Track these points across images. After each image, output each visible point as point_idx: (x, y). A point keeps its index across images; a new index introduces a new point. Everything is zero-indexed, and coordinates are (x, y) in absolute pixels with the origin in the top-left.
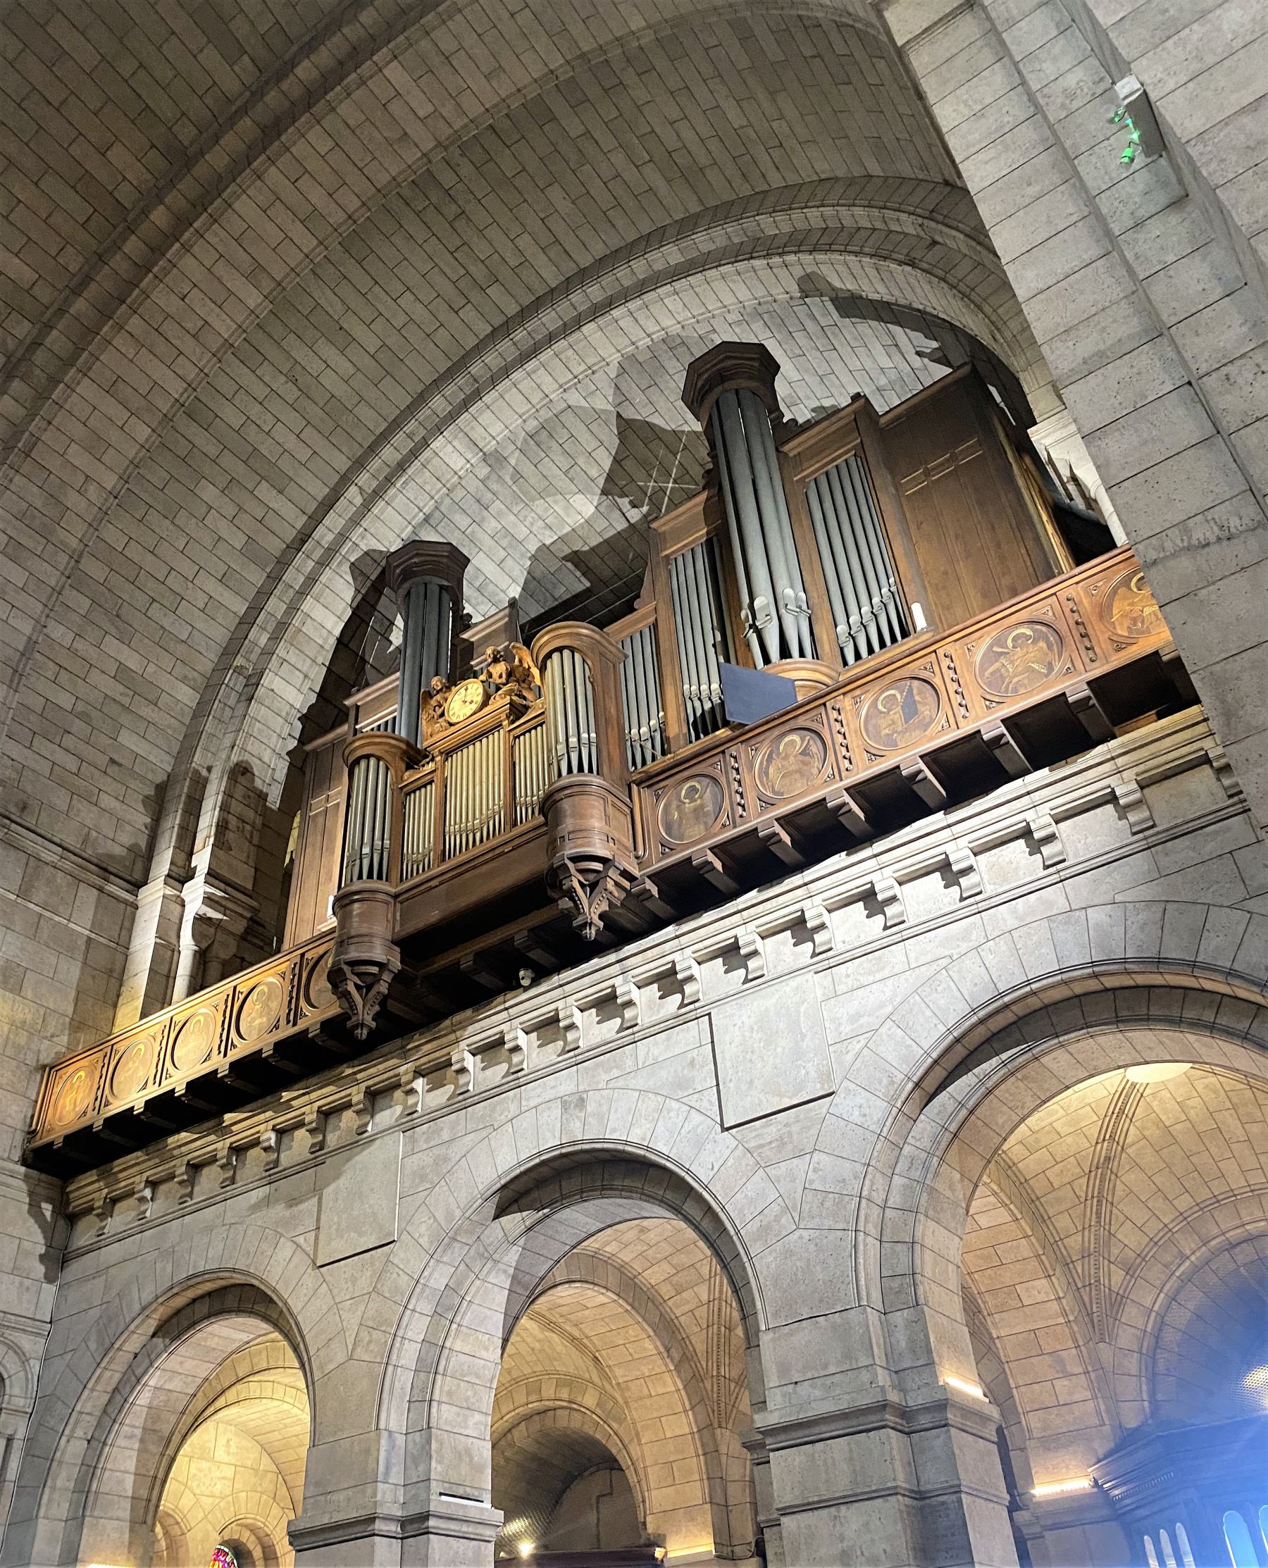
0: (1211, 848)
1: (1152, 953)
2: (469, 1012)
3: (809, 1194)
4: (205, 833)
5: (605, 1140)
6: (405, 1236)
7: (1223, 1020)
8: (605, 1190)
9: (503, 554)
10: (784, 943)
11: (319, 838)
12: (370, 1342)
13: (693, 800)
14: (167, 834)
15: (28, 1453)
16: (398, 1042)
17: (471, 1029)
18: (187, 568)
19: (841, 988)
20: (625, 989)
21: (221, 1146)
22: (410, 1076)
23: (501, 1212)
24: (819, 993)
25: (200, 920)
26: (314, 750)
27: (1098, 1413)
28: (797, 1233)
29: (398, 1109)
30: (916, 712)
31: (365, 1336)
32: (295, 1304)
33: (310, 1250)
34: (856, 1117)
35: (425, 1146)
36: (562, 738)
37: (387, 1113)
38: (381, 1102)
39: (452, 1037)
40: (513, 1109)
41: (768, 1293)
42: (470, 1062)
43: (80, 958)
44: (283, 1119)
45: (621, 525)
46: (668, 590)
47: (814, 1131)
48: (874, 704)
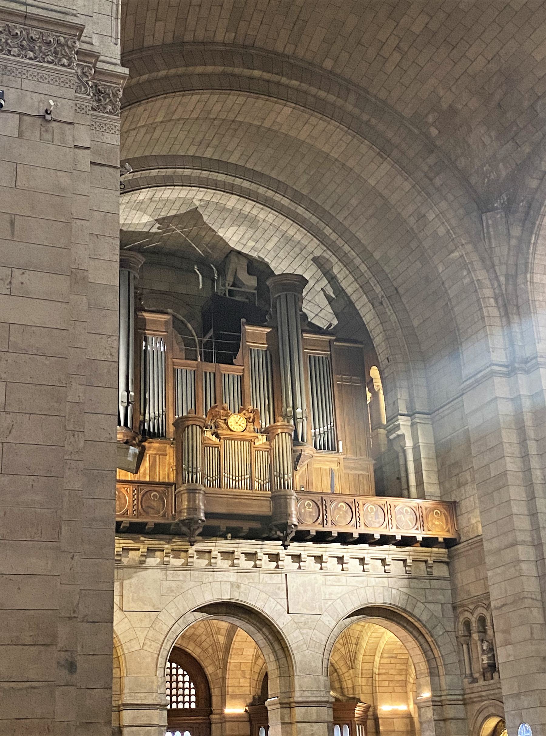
0: (421, 586)
1: (404, 607)
3: (312, 642)
5: (247, 603)
6: (164, 610)
7: (408, 627)
8: (234, 615)
10: (311, 560)
12: (150, 645)
13: (309, 508)
16: (168, 537)
19: (327, 583)
20: (260, 555)
23: (193, 611)
24: (321, 582)
27: (250, 691)
28: (307, 651)
29: (158, 560)
30: (378, 518)
31: (148, 642)
34: (327, 623)
35: (172, 579)
40: (211, 580)
41: (298, 665)
47: (315, 623)
48: (368, 507)
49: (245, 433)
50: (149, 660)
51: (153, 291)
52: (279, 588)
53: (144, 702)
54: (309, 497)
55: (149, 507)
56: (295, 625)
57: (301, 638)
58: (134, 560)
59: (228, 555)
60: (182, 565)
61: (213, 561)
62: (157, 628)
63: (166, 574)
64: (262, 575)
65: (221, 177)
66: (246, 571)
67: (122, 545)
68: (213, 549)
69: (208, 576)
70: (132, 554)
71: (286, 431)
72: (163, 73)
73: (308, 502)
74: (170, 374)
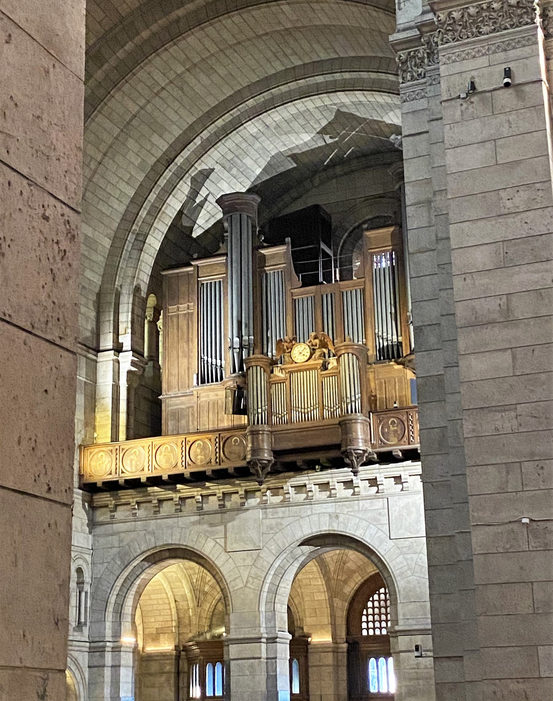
2: (291, 474)
3: (417, 567)
4: (125, 325)
6: (265, 548)
9: (259, 156)
11: (176, 331)
14: (107, 323)
15: (93, 598)
17: (292, 479)
18: (114, 180)
21: (176, 496)
22: (265, 490)
25: (129, 372)
26: (166, 275)
28: (412, 577)
29: (258, 500)
31: (250, 579)
32: (218, 563)
33: (223, 545)
35: (271, 517)
36: (349, 395)
37: (254, 500)
38: (249, 495)
39: (284, 480)
40: (309, 513)
41: (402, 592)
42: (292, 491)
43: (83, 392)
44: (205, 492)
45: (321, 143)
46: (371, 273)
49: (311, 362)
50: (252, 596)
51: (367, 199)
52: (380, 513)
53: (246, 636)
54: (392, 415)
55: (230, 453)
56: (398, 551)
57: (406, 564)
58: (236, 503)
59: (325, 486)
60: (281, 501)
61: (310, 494)
62: (259, 566)
63: (266, 513)
64: (361, 503)
65: (320, 79)
66: (345, 500)
67: (221, 491)
68: (307, 482)
70: (235, 497)
71: (350, 351)
72: (145, 34)
73: (392, 419)
74: (290, 306)
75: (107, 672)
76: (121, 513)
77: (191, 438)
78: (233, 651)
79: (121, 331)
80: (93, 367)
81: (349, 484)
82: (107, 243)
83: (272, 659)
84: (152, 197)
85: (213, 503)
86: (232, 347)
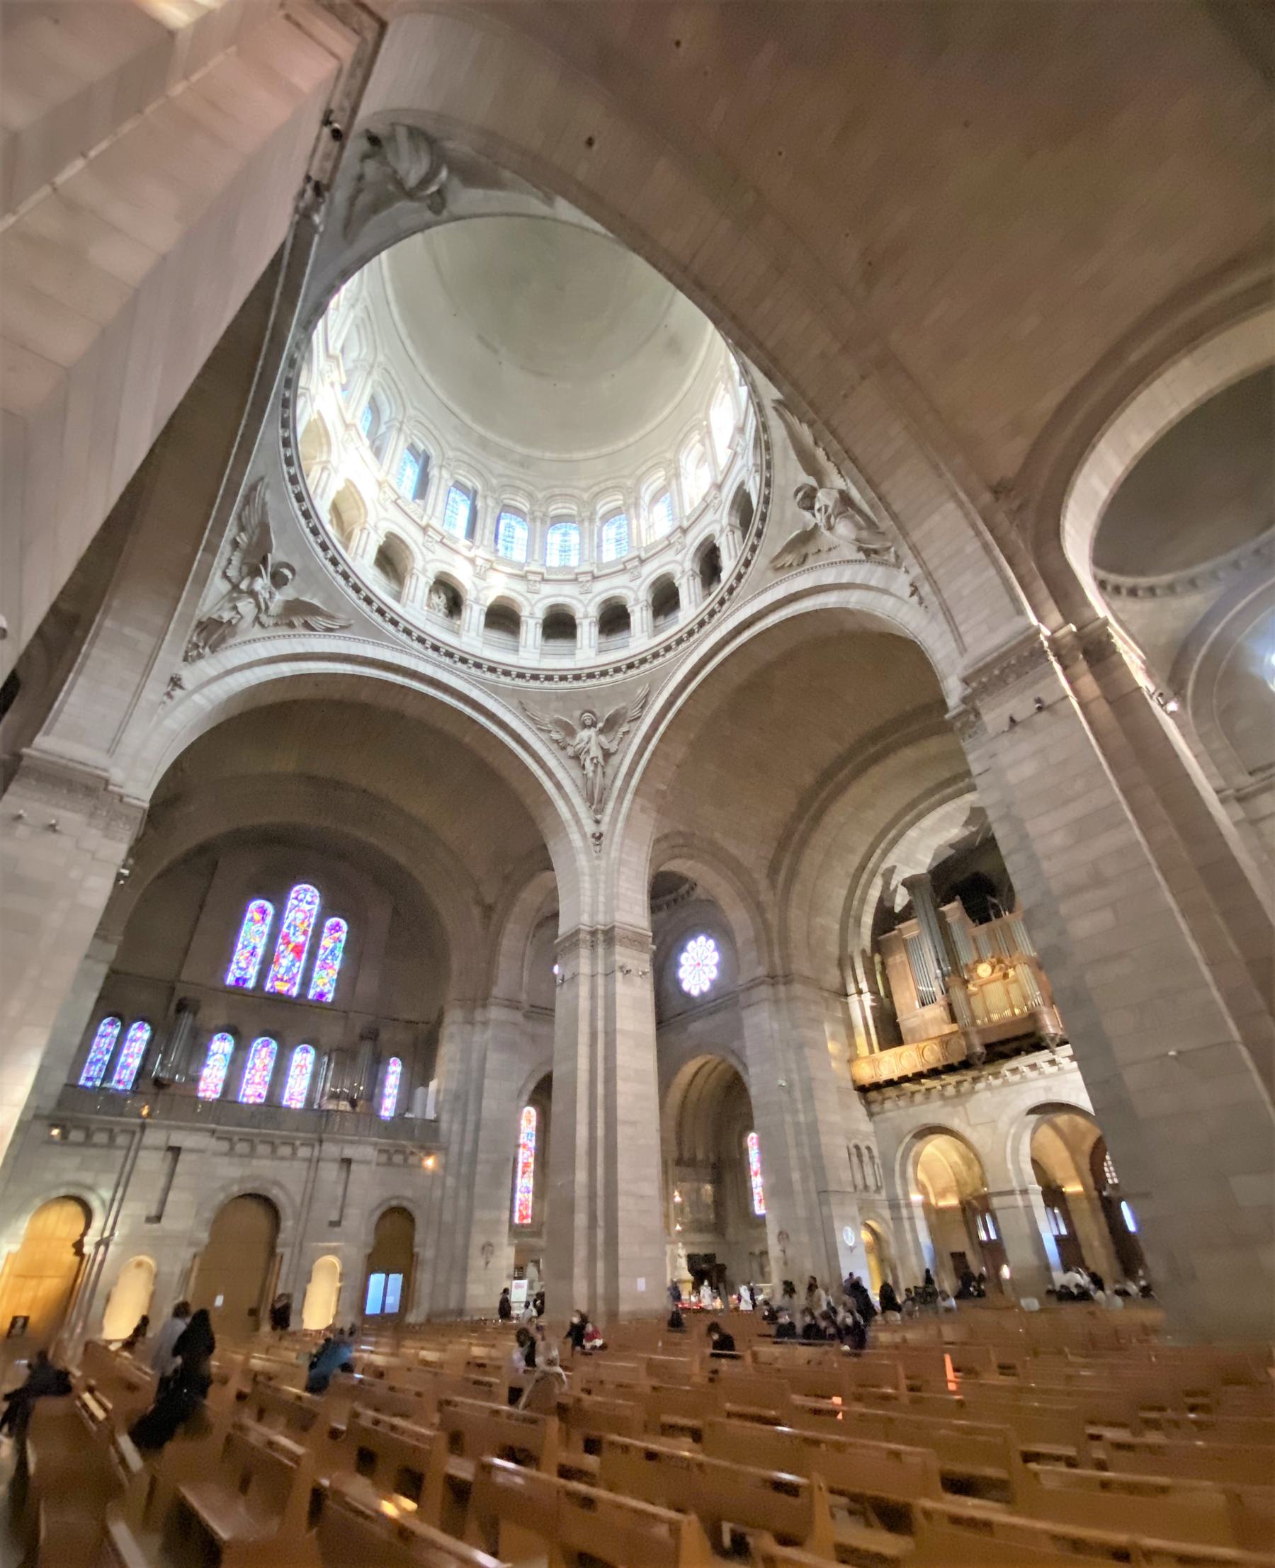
21: (923, 1088)
44: (943, 1083)
59: (1033, 1067)
66: (1051, 1075)
69: (1024, 1087)
75: (906, 1224)
76: (888, 1105)
77: (922, 1045)
78: (995, 1202)
79: (859, 980)
80: (846, 1008)
81: (1052, 1062)
82: (837, 927)
83: (1029, 1208)
84: (858, 893)
85: (950, 1090)
86: (937, 977)
